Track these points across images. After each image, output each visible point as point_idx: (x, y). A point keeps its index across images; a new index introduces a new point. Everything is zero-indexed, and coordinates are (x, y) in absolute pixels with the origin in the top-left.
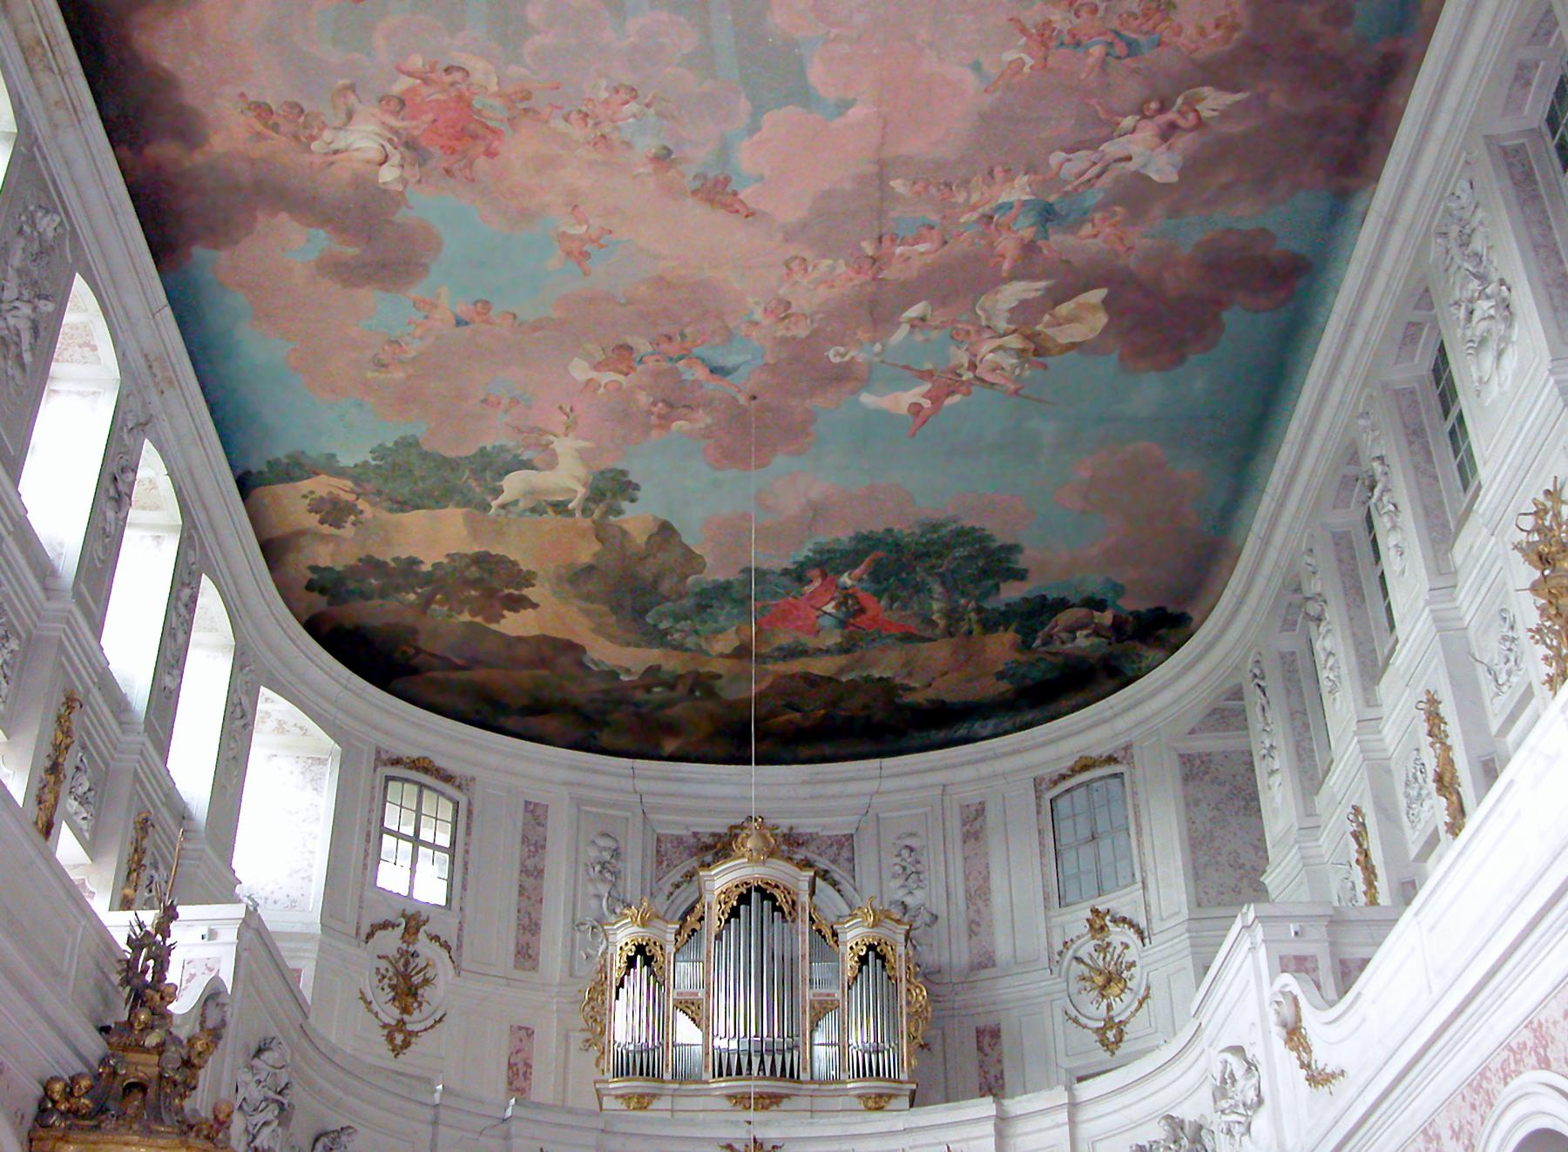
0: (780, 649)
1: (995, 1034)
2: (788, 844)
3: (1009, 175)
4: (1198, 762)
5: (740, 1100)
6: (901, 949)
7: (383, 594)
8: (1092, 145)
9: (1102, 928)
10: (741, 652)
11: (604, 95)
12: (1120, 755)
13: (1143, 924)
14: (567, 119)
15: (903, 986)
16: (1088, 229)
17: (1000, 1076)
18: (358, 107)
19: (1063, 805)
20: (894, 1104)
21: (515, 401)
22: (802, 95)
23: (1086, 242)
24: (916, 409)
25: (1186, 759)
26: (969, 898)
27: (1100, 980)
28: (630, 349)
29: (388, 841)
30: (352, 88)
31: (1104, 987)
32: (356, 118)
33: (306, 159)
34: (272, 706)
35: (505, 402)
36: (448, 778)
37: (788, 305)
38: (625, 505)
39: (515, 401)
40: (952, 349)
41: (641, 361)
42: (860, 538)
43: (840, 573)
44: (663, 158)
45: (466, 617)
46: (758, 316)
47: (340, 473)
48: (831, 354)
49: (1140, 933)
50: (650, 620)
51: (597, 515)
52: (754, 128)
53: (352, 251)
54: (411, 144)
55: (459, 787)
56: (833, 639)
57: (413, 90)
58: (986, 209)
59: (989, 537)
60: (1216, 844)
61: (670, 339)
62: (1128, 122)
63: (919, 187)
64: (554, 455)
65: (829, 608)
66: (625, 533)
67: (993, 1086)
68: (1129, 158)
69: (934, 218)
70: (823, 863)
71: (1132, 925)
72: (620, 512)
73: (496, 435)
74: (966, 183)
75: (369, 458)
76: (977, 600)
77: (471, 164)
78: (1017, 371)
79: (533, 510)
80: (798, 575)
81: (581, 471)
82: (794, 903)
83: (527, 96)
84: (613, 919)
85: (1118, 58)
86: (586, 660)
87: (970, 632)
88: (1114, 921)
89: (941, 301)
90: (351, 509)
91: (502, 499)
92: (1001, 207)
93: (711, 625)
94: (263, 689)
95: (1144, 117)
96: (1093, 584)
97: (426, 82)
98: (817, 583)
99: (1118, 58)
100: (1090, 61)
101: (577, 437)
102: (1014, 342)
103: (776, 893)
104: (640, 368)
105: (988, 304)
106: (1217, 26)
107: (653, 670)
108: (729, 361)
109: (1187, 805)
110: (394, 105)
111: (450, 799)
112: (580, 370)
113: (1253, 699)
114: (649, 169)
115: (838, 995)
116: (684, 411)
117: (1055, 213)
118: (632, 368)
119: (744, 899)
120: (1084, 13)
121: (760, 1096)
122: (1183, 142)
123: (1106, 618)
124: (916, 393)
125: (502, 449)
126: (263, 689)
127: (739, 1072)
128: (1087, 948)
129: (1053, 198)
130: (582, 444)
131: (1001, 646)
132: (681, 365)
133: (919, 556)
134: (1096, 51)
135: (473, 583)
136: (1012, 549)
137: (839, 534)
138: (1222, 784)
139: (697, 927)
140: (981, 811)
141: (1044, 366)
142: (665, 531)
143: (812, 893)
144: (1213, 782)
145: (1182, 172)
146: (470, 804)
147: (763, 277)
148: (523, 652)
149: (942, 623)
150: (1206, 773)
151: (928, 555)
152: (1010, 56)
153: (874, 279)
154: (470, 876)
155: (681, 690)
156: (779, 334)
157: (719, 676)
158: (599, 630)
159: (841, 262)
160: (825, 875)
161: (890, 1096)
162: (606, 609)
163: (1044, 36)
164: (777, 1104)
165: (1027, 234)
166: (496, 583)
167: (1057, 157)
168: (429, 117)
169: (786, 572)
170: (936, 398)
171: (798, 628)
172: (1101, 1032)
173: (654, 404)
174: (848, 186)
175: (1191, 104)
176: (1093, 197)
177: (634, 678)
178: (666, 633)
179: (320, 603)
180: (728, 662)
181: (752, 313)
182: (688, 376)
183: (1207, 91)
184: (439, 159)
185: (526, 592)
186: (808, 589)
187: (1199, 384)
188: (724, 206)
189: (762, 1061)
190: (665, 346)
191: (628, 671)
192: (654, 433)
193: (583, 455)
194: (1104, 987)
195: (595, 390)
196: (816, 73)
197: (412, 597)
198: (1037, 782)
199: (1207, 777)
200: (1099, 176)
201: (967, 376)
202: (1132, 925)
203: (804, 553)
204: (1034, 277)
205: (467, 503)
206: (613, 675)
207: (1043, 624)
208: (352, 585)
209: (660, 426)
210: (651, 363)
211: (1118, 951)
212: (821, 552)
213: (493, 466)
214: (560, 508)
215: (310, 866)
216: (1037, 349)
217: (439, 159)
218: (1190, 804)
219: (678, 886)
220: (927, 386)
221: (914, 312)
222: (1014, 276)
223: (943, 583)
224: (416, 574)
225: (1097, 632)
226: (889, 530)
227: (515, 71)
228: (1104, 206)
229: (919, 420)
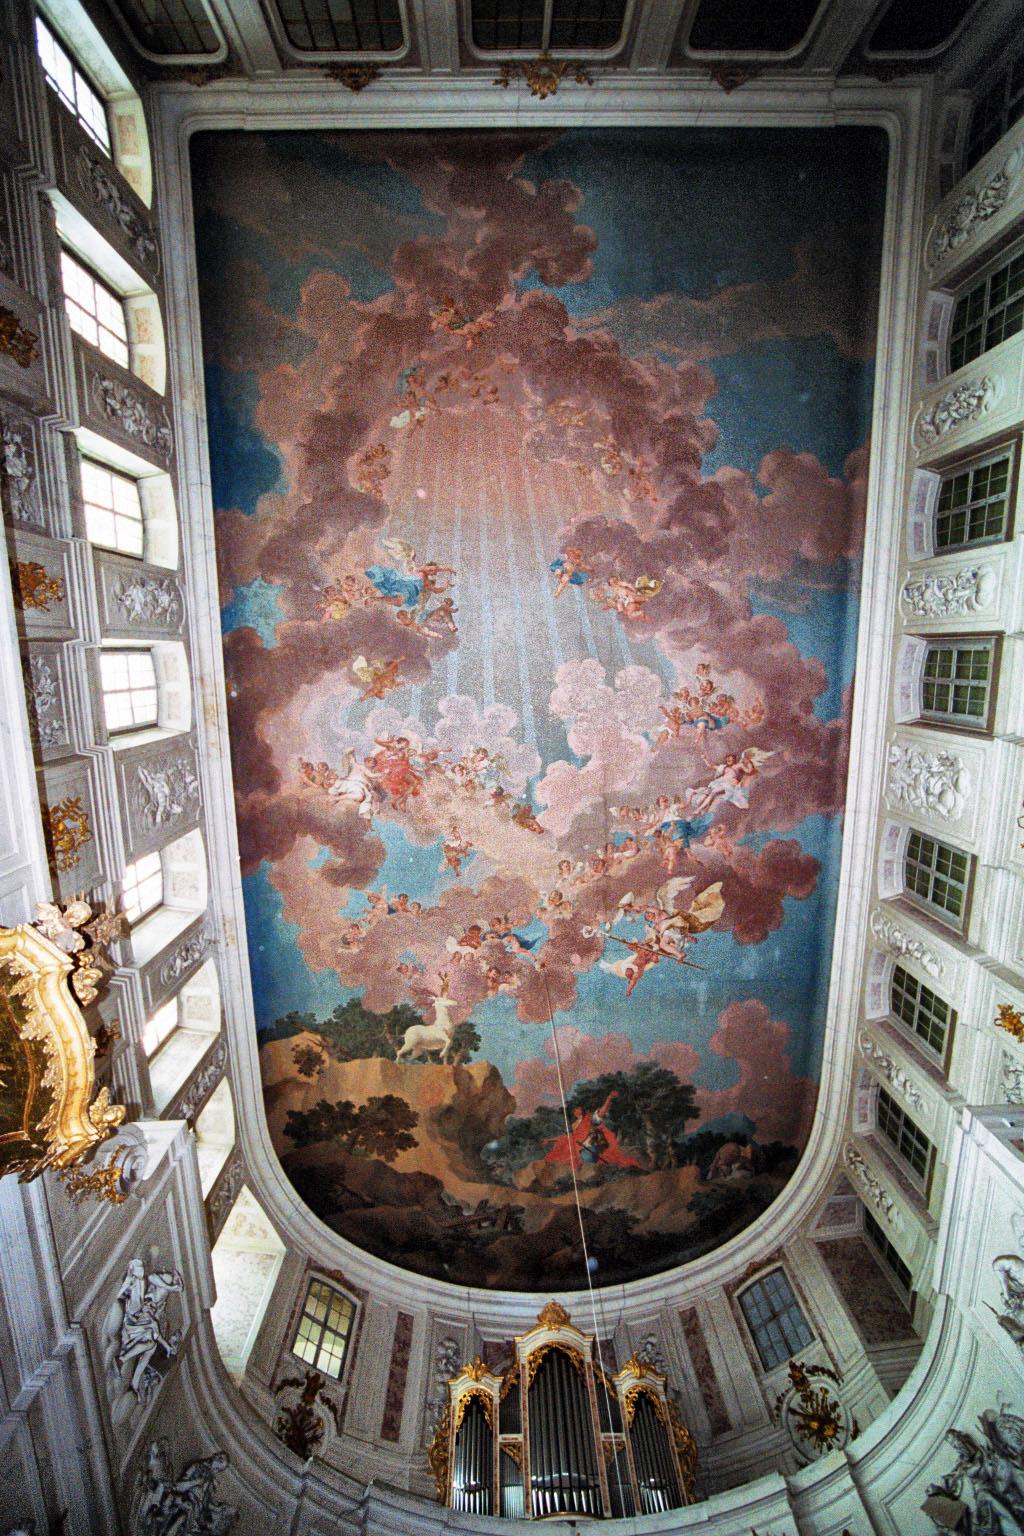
8: (705, 783)
11: (472, 755)
14: (453, 771)
16: (708, 841)
18: (355, 765)
23: (707, 849)
24: (630, 973)
30: (352, 753)
32: (354, 772)
33: (324, 799)
37: (561, 896)
38: (472, 1053)
39: (415, 969)
42: (604, 1079)
43: (592, 1109)
44: (499, 795)
46: (546, 904)
47: (315, 1030)
52: (543, 775)
53: (340, 861)
54: (377, 788)
57: (382, 753)
58: (658, 826)
62: (720, 768)
66: (471, 1077)
68: (723, 792)
69: (632, 833)
72: (467, 1059)
77: (404, 802)
81: (448, 1026)
83: (435, 755)
89: (638, 893)
90: (318, 1060)
91: (405, 1048)
97: (388, 748)
108: (529, 938)
110: (371, 764)
112: (452, 945)
114: (492, 802)
122: (748, 781)
125: (405, 1007)
129: (689, 819)
130: (451, 1003)
132: (505, 941)
134: (701, 725)
135: (381, 1124)
136: (690, 1089)
137: (590, 1076)
141: (696, 940)
142: (494, 1075)
146: (363, 1308)
152: (662, 728)
163: (677, 719)
165: (679, 843)
167: (689, 791)
168: (387, 771)
175: (749, 756)
176: (709, 819)
178: (491, 1169)
183: (755, 750)
184: (391, 796)
188: (529, 827)
192: (490, 993)
196: (573, 742)
204: (686, 874)
209: (494, 988)
213: (403, 1019)
214: (435, 1055)
216: (691, 928)
217: (391, 796)
220: (634, 956)
221: (625, 900)
222: (677, 873)
227: (431, 741)
228: (716, 822)
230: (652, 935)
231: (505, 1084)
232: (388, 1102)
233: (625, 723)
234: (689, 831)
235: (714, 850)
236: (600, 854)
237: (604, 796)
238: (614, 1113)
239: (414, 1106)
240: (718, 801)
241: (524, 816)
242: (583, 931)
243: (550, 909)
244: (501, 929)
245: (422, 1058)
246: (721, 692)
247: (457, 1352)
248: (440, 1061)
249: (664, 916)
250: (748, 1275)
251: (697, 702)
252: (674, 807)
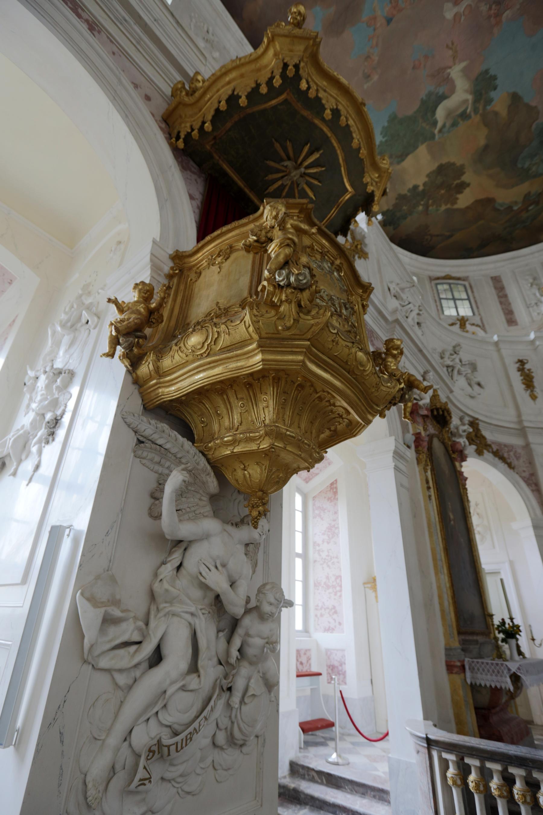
29: (443, 302)
50: (520, 166)
55: (464, 280)
107: (527, 196)
111: (461, 284)
154: (479, 304)
177: (520, 205)
191: (516, 203)
232: (441, 169)
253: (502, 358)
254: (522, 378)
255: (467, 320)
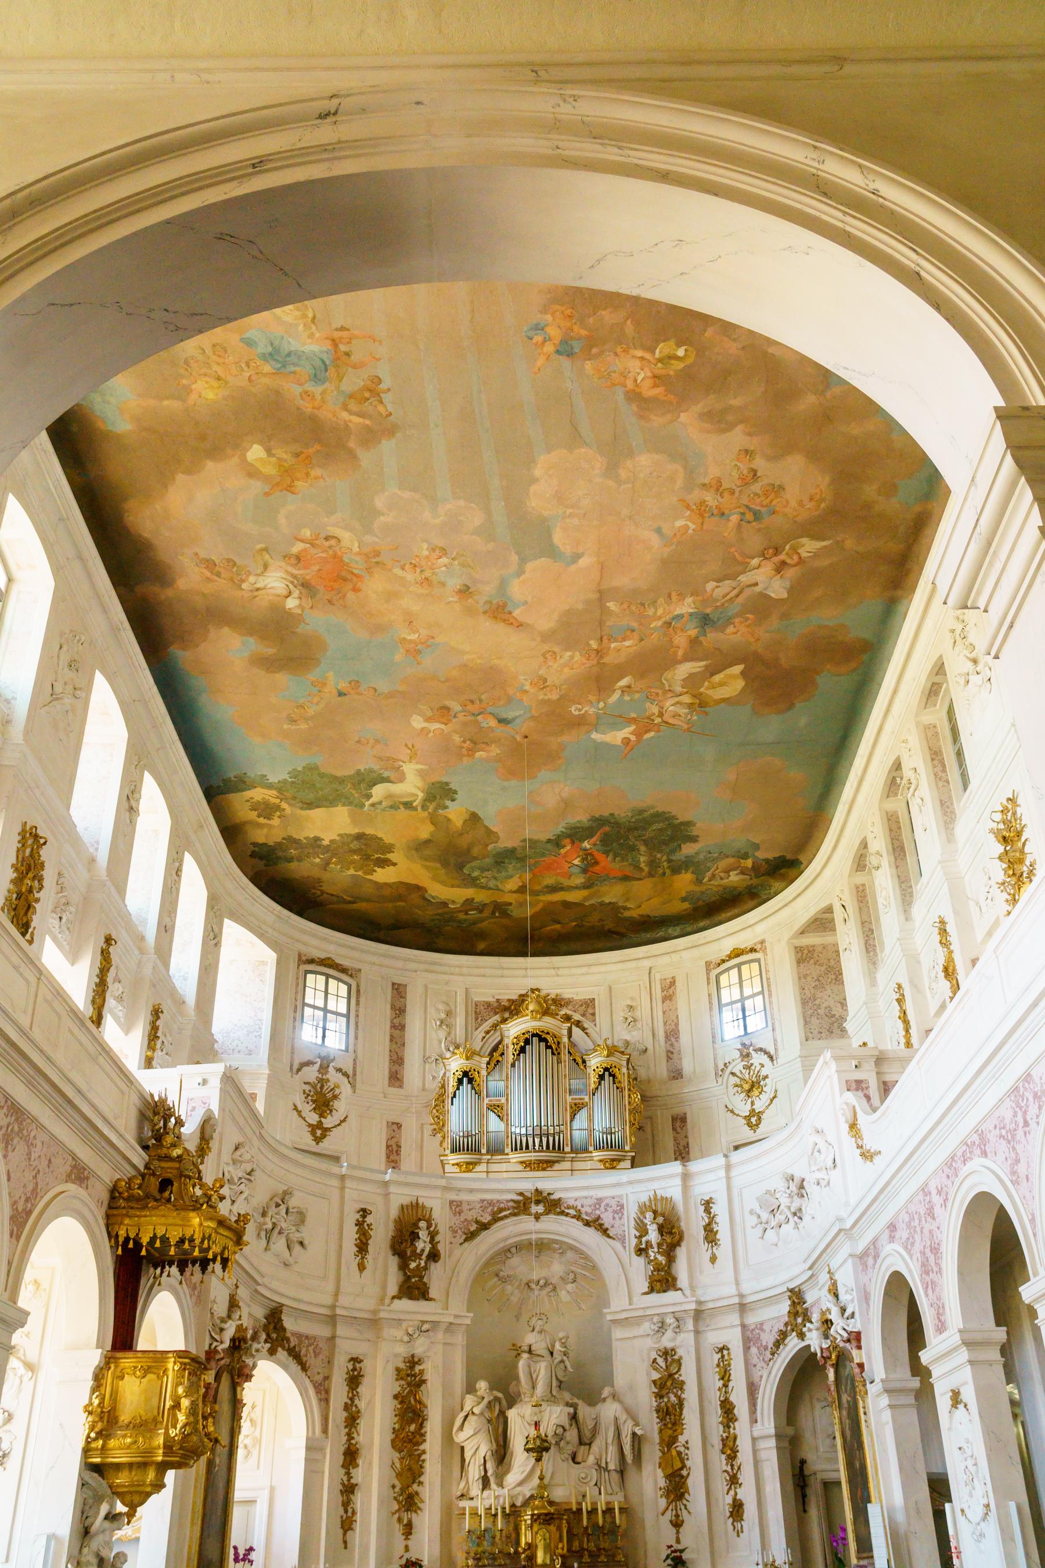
0: (547, 887)
1: (683, 1119)
2: (550, 1006)
3: (682, 596)
4: (806, 952)
5: (528, 1165)
6: (624, 1070)
7: (300, 859)
8: (733, 577)
9: (748, 1055)
10: (522, 890)
12: (758, 947)
13: (772, 1052)
15: (626, 1093)
16: (730, 629)
17: (687, 1146)
19: (724, 979)
20: (622, 1165)
21: (377, 741)
22: (551, 551)
24: (626, 741)
25: (799, 950)
26: (667, 1037)
27: (747, 1087)
28: (448, 709)
31: (749, 1091)
34: (232, 931)
35: (372, 741)
36: (344, 970)
37: (545, 680)
38: (448, 803)
40: (648, 704)
41: (455, 716)
42: (594, 819)
43: (582, 840)
45: (352, 872)
46: (527, 687)
48: (573, 709)
49: (771, 1058)
50: (466, 871)
51: (430, 810)
56: (579, 880)
58: (668, 618)
59: (674, 817)
60: (817, 1002)
61: (472, 702)
62: (755, 562)
63: (625, 606)
64: (403, 774)
65: (576, 862)
66: (449, 820)
67: (682, 1154)
68: (756, 584)
69: (635, 625)
70: (577, 1017)
71: (766, 1052)
72: (446, 807)
73: (366, 763)
74: (654, 603)
75: (287, 777)
76: (668, 855)
78: (689, 717)
79: (391, 807)
80: (556, 843)
81: (420, 784)
82: (559, 1043)
84: (448, 1055)
85: (749, 522)
86: (426, 895)
87: (664, 874)
88: (755, 1050)
89: (641, 675)
90: (278, 808)
91: (371, 801)
92: (678, 616)
93: (504, 874)
94: (227, 922)
95: (766, 558)
96: (740, 842)
98: (568, 848)
99: (749, 522)
100: (731, 525)
101: (417, 763)
102: (687, 699)
103: (549, 1038)
104: (454, 720)
105: (669, 676)
106: (811, 499)
108: (510, 715)
109: (800, 978)
112: (417, 722)
113: (838, 914)
115: (587, 1099)
116: (483, 746)
117: (710, 620)
118: (450, 721)
119: (527, 1042)
120: (726, 495)
121: (541, 1161)
122: (791, 573)
123: (749, 863)
124: (627, 732)
125: (371, 771)
126: (227, 922)
127: (527, 1147)
128: (738, 1067)
129: (708, 611)
131: (684, 882)
132: (479, 718)
133: (630, 830)
136: (689, 824)
137: (580, 817)
138: (821, 965)
139: (500, 1059)
140: (673, 983)
141: (706, 713)
142: (474, 818)
143: (570, 1035)
144: (815, 964)
145: (790, 591)
147: (530, 665)
148: (387, 892)
149: (646, 869)
150: (811, 958)
151: (636, 829)
153: (598, 663)
155: (486, 913)
156: (540, 697)
157: (510, 904)
158: (435, 878)
159: (577, 653)
160: (578, 1024)
161: (619, 1161)
162: (439, 865)
163: (701, 511)
164: (551, 1166)
165: (693, 633)
166: (370, 850)
167: (710, 586)
169: (549, 841)
170: (639, 734)
171: (558, 874)
172: (747, 1118)
173: (464, 742)
174: (580, 606)
175: (794, 550)
176: (735, 608)
179: (260, 865)
180: (515, 895)
181: (523, 685)
182: (484, 725)
183: (804, 540)
185: (388, 856)
186: (563, 851)
187: (803, 721)
188: (504, 621)
189: (541, 1141)
190: (470, 707)
193: (421, 774)
194: (749, 1091)
195: (428, 734)
197: (317, 860)
198: (708, 964)
199: (812, 961)
200: (737, 596)
201: (658, 720)
202: (766, 1052)
203: (560, 828)
205: (350, 804)
206: (445, 904)
207: (709, 869)
208: (280, 854)
209: (468, 755)
210: (461, 717)
211: (757, 1069)
212: (571, 829)
213: (368, 780)
214: (408, 805)
215: (260, 1028)
216: (701, 704)
218: (802, 977)
219: (488, 1032)
220: (633, 728)
221: (624, 682)
222: (686, 659)
223: (646, 845)
224: (319, 846)
225: (742, 873)
226: (612, 815)
229: (629, 748)
230: (655, 710)
231: (486, 823)
233: (630, 518)
234: (705, 621)
235: (737, 638)
236: (594, 645)
237: (600, 591)
238: (606, 841)
239: (388, 839)
240: (748, 592)
241: (499, 611)
242: (573, 709)
243: (532, 691)
244: (474, 708)
245: (393, 807)
246: (766, 481)
247: (449, 1014)
248: (415, 809)
249: (669, 695)
250: (730, 957)
251: (732, 493)
252: (689, 600)
253: (342, 1198)
254: (357, 1236)
255: (332, 1061)
